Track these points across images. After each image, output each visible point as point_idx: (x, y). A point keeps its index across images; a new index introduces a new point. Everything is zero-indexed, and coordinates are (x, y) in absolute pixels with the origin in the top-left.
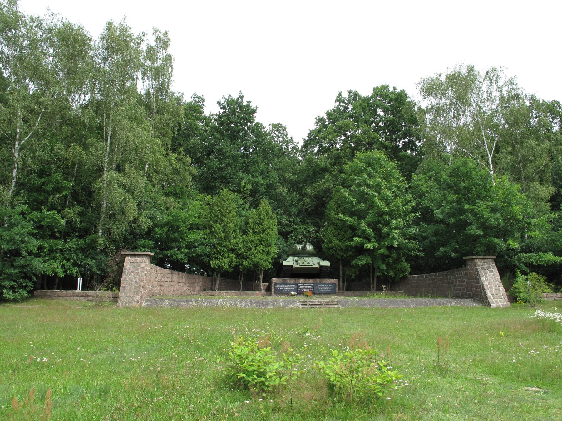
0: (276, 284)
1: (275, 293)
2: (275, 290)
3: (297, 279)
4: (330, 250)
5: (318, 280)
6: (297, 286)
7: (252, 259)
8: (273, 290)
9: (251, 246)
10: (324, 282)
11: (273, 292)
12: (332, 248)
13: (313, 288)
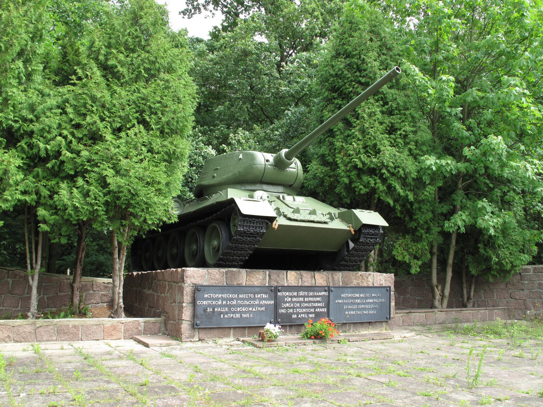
0: (197, 289)
1: (194, 326)
2: (194, 316)
3: (275, 273)
4: (365, 178)
5: (339, 277)
6: (276, 298)
7: (103, 182)
8: (187, 314)
9: (101, 125)
10: (355, 283)
11: (185, 326)
12: (372, 171)
13: (328, 306)
